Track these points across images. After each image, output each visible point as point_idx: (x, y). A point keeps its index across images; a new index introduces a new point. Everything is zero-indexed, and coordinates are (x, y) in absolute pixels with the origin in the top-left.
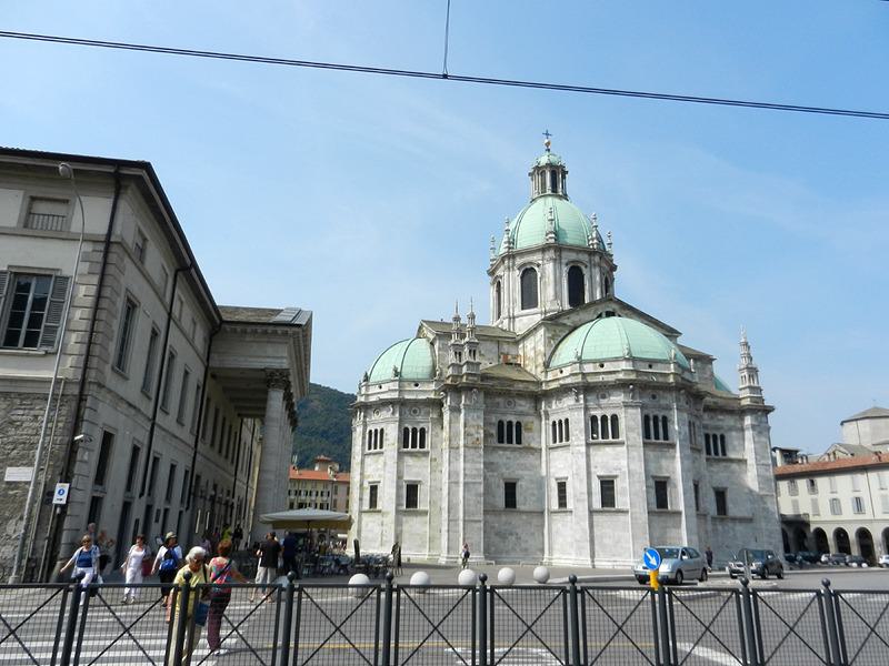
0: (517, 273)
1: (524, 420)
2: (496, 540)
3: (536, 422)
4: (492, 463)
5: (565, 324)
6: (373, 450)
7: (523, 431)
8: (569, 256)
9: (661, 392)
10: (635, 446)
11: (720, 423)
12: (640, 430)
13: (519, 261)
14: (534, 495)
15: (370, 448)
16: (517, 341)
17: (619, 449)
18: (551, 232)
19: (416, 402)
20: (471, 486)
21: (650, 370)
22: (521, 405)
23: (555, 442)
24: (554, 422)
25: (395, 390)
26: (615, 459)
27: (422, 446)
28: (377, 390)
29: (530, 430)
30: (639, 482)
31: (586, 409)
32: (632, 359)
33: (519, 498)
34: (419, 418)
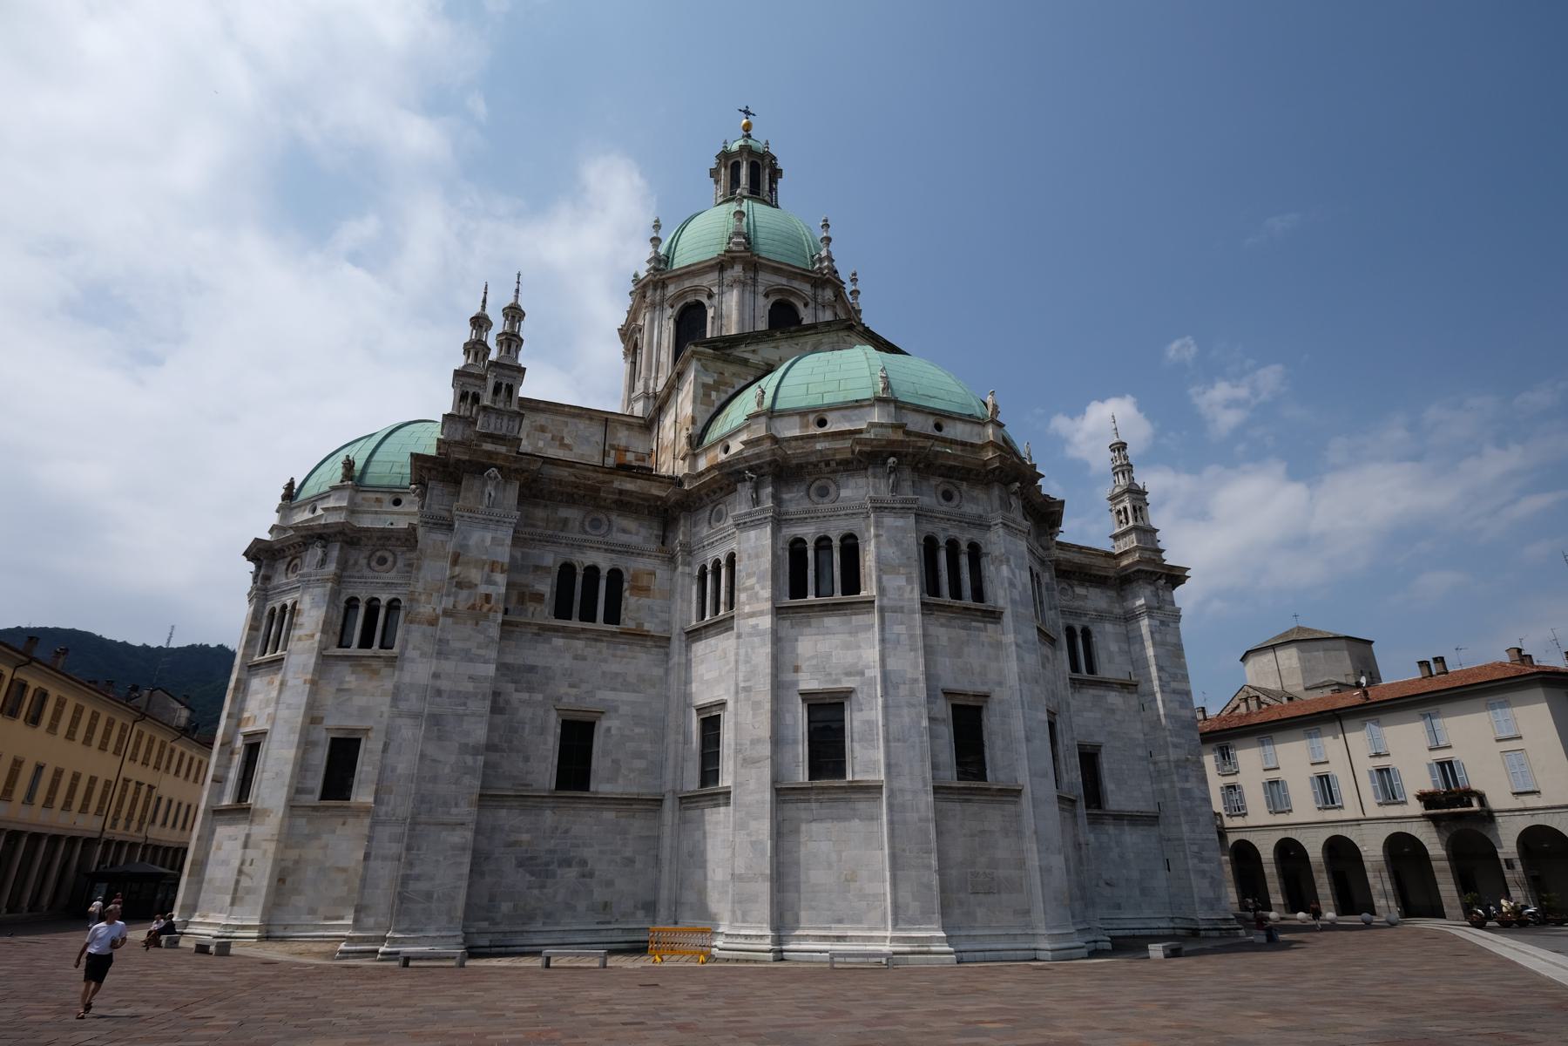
0: (669, 312)
1: (630, 566)
3: (662, 573)
4: (532, 669)
7: (626, 594)
9: (964, 486)
10: (901, 610)
11: (1081, 603)
12: (916, 572)
14: (639, 755)
16: (649, 425)
18: (737, 234)
19: (387, 538)
21: (937, 434)
22: (624, 531)
23: (703, 617)
28: (307, 515)
31: (778, 521)
32: (900, 406)
33: (599, 763)
34: (391, 576)
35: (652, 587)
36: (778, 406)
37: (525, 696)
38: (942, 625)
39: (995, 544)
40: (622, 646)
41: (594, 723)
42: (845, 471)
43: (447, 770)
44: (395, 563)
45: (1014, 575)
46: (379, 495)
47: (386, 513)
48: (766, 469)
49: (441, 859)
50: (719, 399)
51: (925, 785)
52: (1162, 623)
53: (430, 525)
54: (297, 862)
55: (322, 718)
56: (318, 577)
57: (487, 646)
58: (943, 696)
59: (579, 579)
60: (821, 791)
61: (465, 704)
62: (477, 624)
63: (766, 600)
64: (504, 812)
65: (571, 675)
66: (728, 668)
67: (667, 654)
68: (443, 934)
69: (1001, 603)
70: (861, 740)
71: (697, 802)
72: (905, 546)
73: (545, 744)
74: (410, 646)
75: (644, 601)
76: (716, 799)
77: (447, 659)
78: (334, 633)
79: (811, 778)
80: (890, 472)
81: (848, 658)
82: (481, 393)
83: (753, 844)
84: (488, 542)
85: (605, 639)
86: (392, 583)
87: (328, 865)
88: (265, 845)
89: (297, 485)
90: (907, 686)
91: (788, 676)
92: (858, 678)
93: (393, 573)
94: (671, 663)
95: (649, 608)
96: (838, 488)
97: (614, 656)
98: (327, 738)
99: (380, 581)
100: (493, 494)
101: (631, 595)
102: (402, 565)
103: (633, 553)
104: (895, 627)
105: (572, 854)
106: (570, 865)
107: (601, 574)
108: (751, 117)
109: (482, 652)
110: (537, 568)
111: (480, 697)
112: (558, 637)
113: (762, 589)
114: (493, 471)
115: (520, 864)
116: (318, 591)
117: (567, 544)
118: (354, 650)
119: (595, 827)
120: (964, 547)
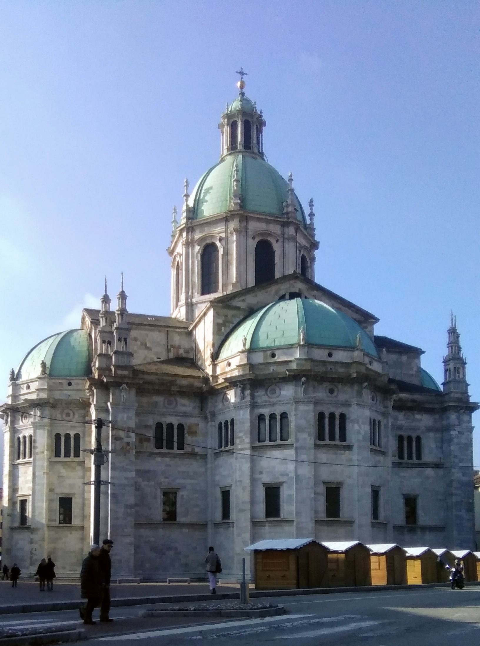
1: (187, 422)
3: (202, 424)
4: (148, 471)
7: (186, 435)
22: (184, 405)
23: (221, 446)
29: (193, 433)
31: (253, 406)
37: (147, 483)
44: (74, 415)
45: (360, 427)
46: (60, 381)
47: (66, 390)
48: (246, 382)
51: (312, 519)
58: (322, 483)
62: (125, 456)
64: (142, 530)
75: (194, 438)
84: (125, 418)
89: (16, 372)
91: (258, 476)
101: (189, 435)
103: (188, 416)
107: (174, 427)
110: (146, 426)
113: (246, 438)
114: (124, 386)
120: (338, 417)
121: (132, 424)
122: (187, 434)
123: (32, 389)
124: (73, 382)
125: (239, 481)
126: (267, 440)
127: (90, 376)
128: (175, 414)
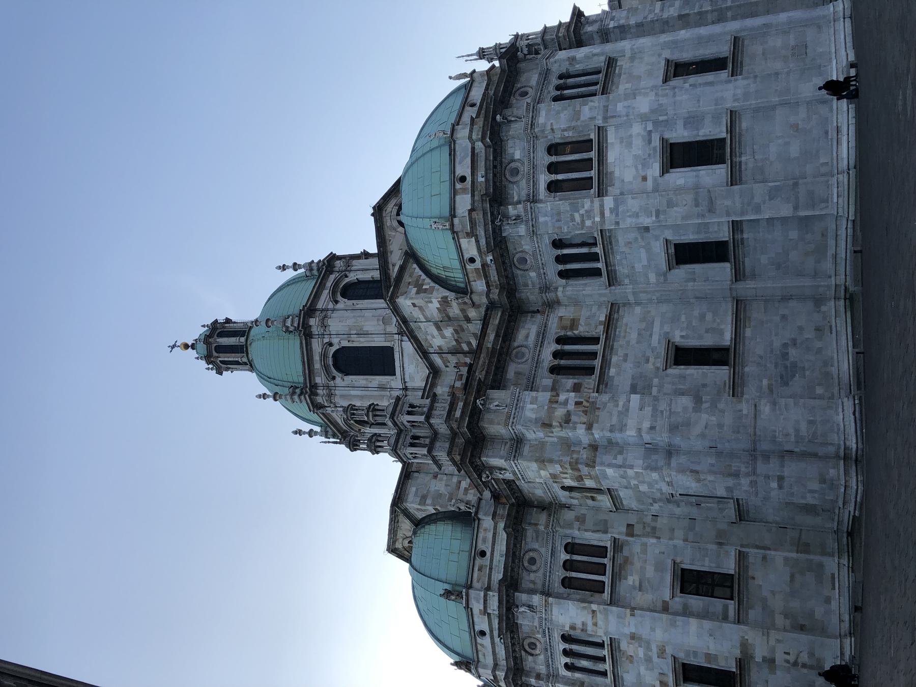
1: (554, 329)
2: (797, 384)
3: (561, 312)
5: (402, 269)
6: (607, 666)
7: (576, 332)
8: (324, 301)
10: (606, 109)
13: (318, 380)
14: (702, 317)
15: (604, 674)
17: (611, 137)
19: (514, 555)
20: (672, 420)
21: (478, 104)
22: (527, 337)
24: (563, 274)
25: (485, 596)
26: (629, 145)
27: (601, 551)
29: (574, 323)
30: (674, 95)
33: (708, 341)
34: (545, 551)
35: (571, 317)
36: (447, 214)
37: (655, 391)
38: (617, 88)
39: (560, 66)
40: (617, 333)
41: (676, 346)
42: (501, 156)
43: (714, 418)
46: (476, 569)
49: (782, 417)
50: (429, 284)
51: (730, 81)
52: (612, 19)
53: (517, 455)
54: (786, 616)
55: (664, 602)
56: (544, 611)
57: (617, 401)
59: (563, 362)
60: (734, 154)
61: (662, 412)
62: (599, 409)
63: (592, 202)
65: (639, 362)
66: (640, 239)
67: (624, 305)
68: (840, 410)
69: (603, 58)
70: (698, 129)
71: (739, 264)
72: (560, 108)
73: (693, 375)
74: (614, 461)
75: (582, 322)
76: (738, 240)
77: (626, 425)
78: (592, 596)
79: (724, 162)
80: (506, 119)
81: (638, 143)
82: (412, 434)
83: (771, 199)
84: (535, 406)
85: (611, 343)
86: (552, 550)
87: (788, 590)
88: (772, 642)
89: (458, 659)
90: (660, 98)
92: (653, 135)
93: (543, 550)
94: (631, 298)
95: (588, 318)
96: (513, 161)
97: (624, 337)
98: (680, 597)
99: (549, 560)
100: (496, 403)
102: (537, 544)
103: (544, 330)
104: (618, 109)
105: (778, 352)
106: (787, 353)
108: (178, 344)
109: (621, 403)
111: (656, 403)
112: (609, 372)
115: (786, 384)
116: (555, 610)
117: (535, 371)
118: (606, 579)
119: (758, 340)
121: (544, 397)
122: (574, 332)
123: (485, 628)
124: (481, 547)
125: (657, 216)
126: (590, 174)
127: (473, 515)
128: (538, 348)
